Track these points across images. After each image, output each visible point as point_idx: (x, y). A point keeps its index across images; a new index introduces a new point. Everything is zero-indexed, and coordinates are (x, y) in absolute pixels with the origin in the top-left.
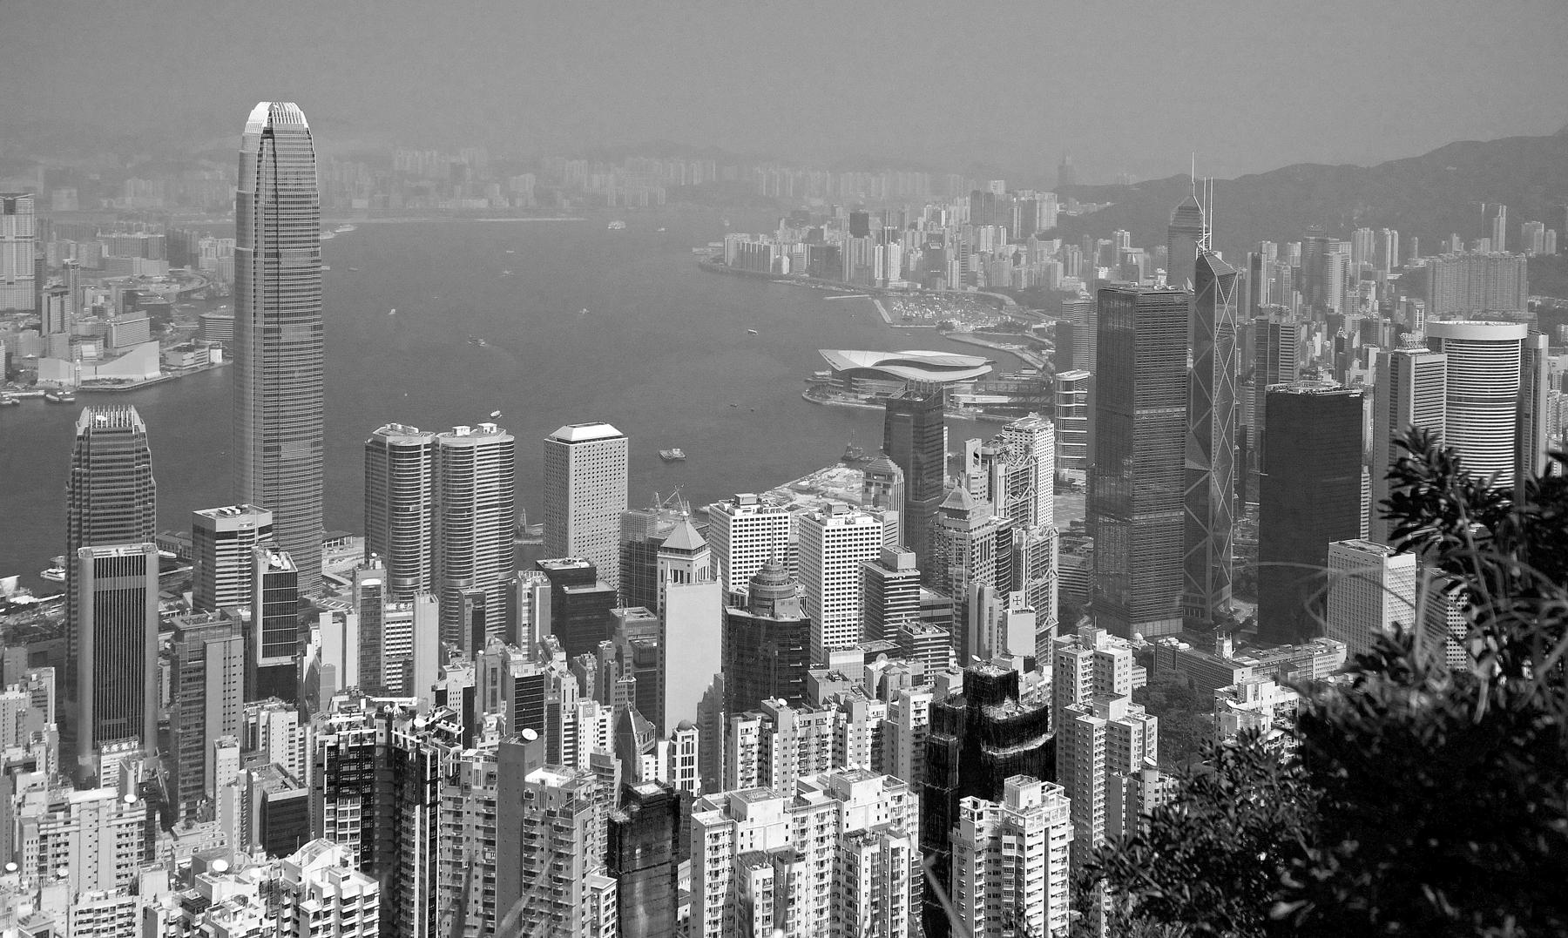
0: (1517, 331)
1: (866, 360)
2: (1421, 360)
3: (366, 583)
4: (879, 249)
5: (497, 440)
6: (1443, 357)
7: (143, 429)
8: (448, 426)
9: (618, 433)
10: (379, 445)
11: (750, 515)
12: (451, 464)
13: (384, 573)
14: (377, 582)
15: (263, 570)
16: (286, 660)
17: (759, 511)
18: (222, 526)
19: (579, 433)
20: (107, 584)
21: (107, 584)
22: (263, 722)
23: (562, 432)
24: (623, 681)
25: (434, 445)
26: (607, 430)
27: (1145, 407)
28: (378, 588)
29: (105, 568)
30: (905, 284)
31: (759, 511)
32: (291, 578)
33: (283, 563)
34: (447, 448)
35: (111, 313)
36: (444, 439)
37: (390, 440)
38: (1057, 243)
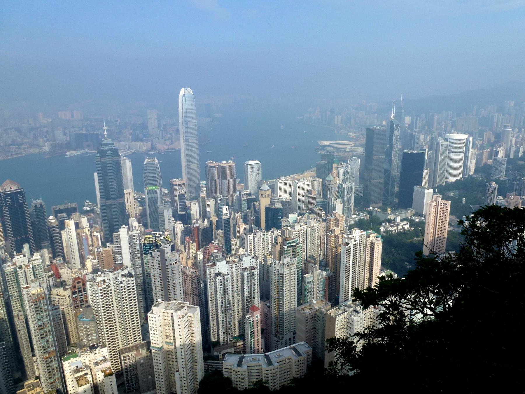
0: (465, 137)
1: (327, 143)
2: (443, 143)
3: (202, 196)
4: (336, 117)
5: (232, 164)
6: (448, 143)
7: (157, 163)
8: (221, 161)
9: (259, 162)
10: (207, 166)
11: (282, 182)
12: (222, 169)
13: (206, 194)
14: (204, 196)
15: (178, 194)
16: (184, 212)
17: (285, 181)
18: (174, 183)
19: (250, 162)
20: (150, 196)
21: (150, 196)
22: (176, 226)
23: (246, 162)
24: (252, 218)
25: (218, 165)
26: (257, 162)
27: (375, 156)
28: (205, 197)
29: (149, 192)
30: (342, 125)
31: (285, 181)
32: (184, 195)
33: (183, 192)
34: (221, 166)
35: (173, 134)
36: (221, 164)
37: (209, 164)
38: (376, 115)
